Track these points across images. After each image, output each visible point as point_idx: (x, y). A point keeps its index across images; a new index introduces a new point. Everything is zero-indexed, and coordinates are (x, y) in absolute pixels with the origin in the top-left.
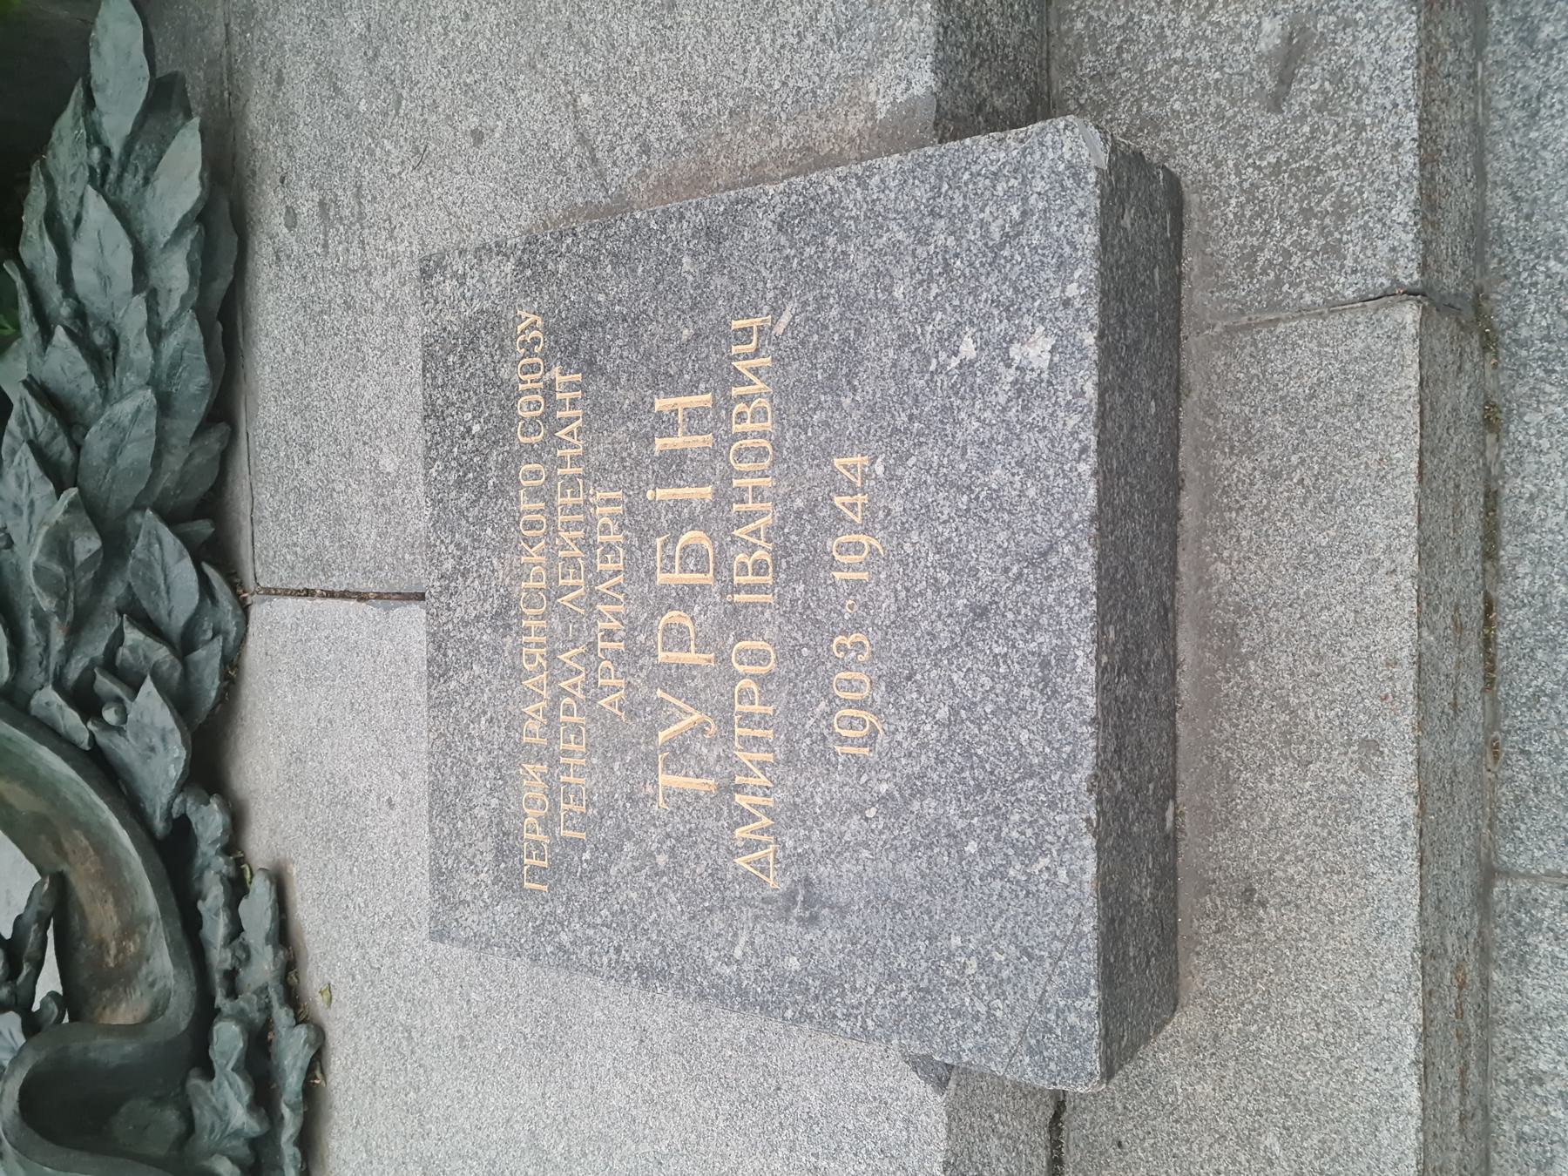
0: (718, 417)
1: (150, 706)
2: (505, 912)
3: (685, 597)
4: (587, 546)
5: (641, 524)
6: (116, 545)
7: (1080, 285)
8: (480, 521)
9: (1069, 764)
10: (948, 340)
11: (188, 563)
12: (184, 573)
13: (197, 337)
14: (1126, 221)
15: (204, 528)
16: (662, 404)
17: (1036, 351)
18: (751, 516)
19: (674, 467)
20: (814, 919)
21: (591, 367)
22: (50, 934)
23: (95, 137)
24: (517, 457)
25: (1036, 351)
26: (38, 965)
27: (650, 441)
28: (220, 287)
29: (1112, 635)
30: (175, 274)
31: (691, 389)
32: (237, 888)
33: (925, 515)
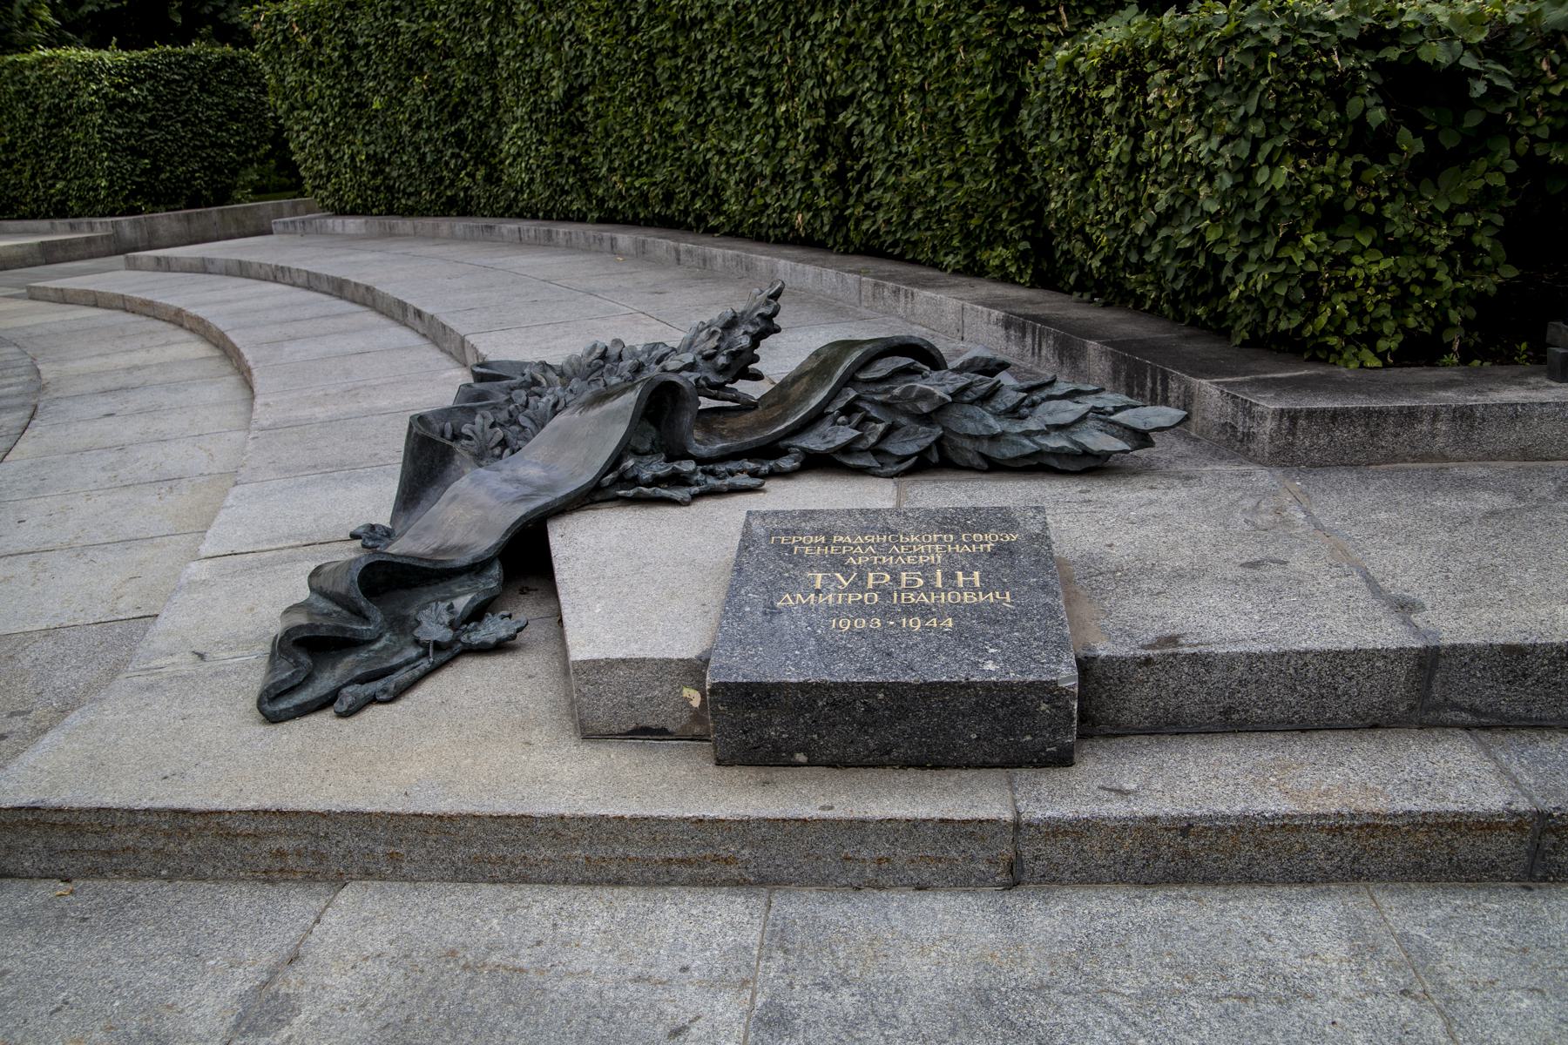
0: (969, 586)
1: (845, 434)
2: (762, 532)
3: (896, 580)
4: (918, 554)
5: (926, 569)
6: (926, 419)
7: (1014, 676)
8: (928, 524)
9: (831, 675)
10: (996, 646)
11: (917, 450)
12: (912, 448)
13: (1028, 451)
14: (1044, 707)
15: (935, 458)
16: (976, 574)
17: (990, 666)
18: (929, 597)
19: (950, 576)
20: (765, 613)
21: (992, 554)
22: (728, 404)
23: (1117, 410)
24: (956, 534)
25: (990, 666)
26: (715, 398)
27: (962, 569)
28: (1055, 463)
29: (881, 696)
30: (1055, 442)
31: (981, 581)
32: (753, 474)
33: (927, 641)
